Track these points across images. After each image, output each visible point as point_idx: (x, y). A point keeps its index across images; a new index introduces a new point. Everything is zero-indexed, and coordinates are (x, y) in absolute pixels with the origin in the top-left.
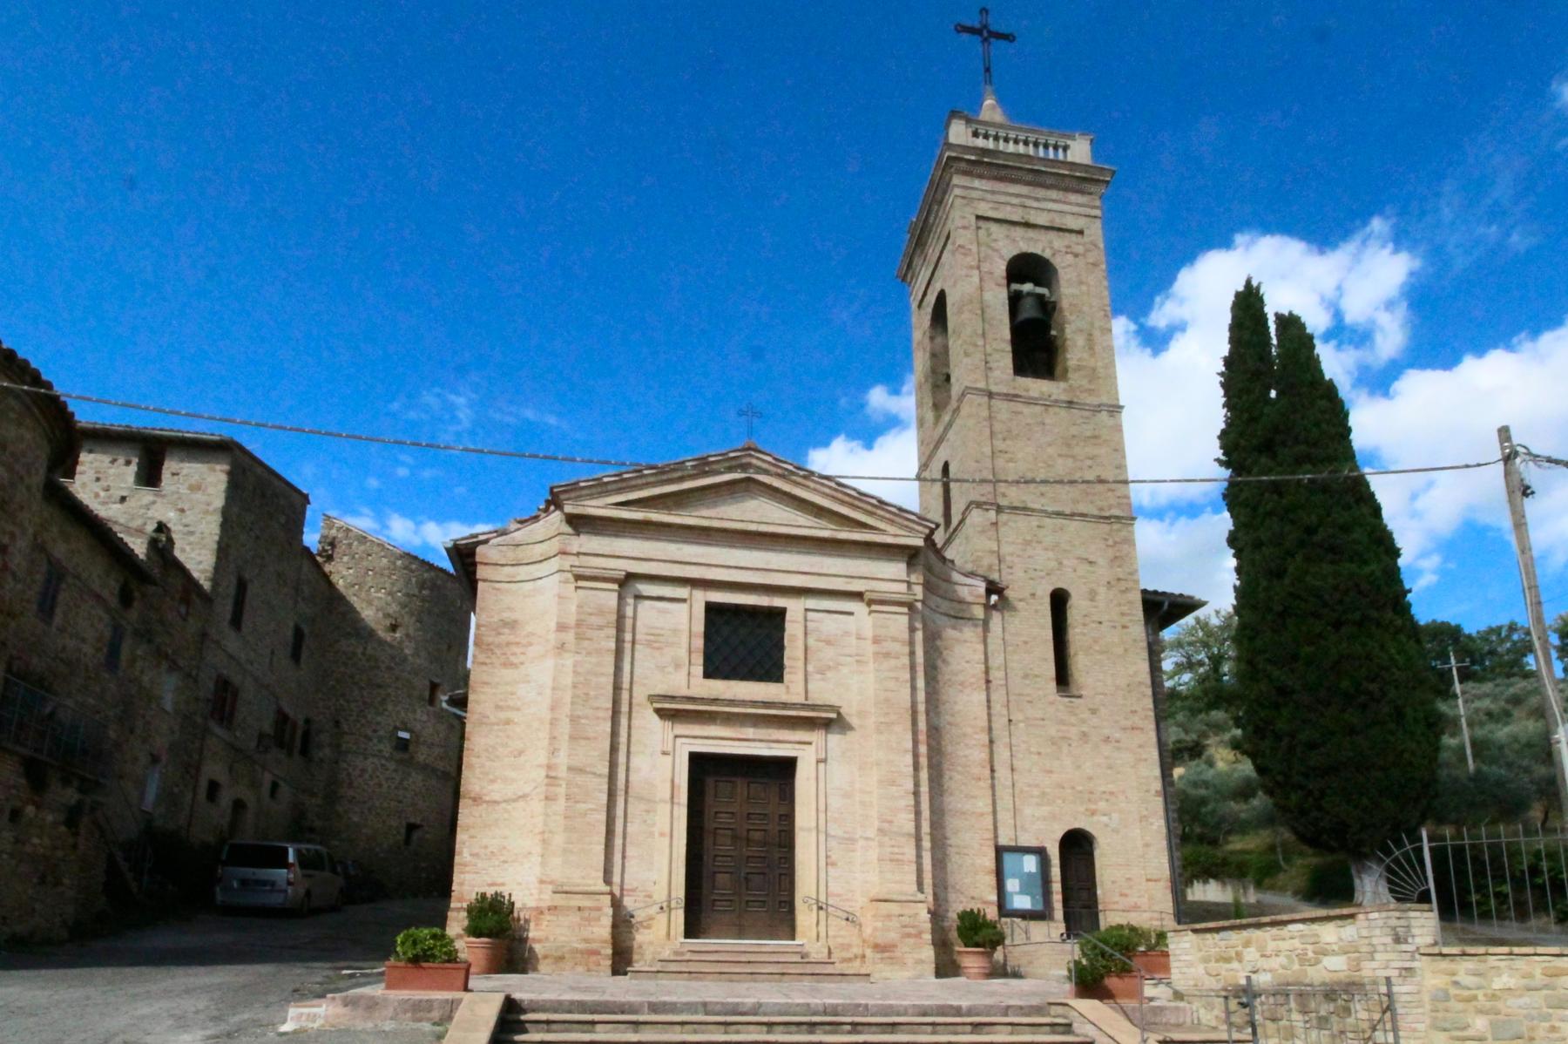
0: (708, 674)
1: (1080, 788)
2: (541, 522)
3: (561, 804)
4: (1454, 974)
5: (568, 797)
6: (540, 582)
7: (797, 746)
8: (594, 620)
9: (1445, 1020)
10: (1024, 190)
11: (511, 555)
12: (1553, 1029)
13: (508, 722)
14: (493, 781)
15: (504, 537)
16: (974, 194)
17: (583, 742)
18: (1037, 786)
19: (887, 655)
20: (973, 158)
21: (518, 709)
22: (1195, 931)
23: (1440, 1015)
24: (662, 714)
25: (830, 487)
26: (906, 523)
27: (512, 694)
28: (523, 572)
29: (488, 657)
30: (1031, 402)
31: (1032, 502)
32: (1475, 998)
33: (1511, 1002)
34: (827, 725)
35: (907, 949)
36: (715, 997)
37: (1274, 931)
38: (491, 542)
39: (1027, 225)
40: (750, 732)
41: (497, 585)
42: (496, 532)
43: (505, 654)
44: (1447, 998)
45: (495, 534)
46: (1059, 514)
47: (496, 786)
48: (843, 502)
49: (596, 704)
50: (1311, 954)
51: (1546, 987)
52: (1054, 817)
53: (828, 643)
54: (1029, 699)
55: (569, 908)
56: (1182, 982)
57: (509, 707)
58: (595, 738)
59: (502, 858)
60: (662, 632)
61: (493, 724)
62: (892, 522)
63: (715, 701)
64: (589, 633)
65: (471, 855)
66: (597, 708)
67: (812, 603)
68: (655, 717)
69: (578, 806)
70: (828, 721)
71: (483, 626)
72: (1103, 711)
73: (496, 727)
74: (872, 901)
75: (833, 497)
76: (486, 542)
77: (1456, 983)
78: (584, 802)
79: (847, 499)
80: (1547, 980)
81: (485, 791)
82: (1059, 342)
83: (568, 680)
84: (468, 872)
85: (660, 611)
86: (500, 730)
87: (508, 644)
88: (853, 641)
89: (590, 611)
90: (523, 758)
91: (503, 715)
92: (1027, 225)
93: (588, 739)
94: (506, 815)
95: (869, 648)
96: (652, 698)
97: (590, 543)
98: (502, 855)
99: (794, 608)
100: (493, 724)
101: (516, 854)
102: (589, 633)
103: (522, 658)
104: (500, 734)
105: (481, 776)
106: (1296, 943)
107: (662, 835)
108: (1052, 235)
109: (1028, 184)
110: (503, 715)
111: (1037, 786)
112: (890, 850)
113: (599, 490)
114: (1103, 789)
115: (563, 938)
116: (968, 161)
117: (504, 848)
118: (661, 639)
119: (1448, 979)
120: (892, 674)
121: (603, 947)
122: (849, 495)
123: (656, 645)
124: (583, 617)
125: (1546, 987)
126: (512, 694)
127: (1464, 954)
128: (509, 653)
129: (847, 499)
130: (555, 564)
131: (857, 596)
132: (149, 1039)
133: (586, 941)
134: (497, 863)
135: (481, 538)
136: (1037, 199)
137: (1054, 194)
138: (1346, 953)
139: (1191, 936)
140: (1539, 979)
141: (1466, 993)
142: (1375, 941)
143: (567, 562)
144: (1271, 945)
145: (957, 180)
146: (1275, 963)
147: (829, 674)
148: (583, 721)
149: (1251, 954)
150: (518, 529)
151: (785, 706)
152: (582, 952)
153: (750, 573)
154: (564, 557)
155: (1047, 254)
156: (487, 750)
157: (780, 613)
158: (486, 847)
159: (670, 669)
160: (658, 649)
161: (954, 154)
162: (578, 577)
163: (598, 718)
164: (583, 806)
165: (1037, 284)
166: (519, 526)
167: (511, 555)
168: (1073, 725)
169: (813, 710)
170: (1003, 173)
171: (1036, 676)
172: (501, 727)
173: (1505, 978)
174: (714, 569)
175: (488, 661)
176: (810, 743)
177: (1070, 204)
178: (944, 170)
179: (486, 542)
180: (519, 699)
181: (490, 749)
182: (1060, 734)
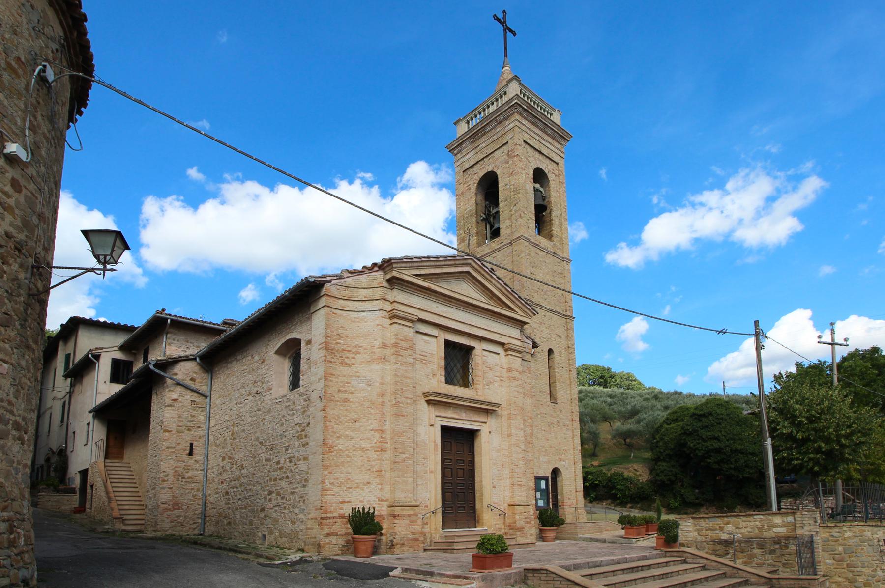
0: (447, 382)
1: (557, 448)
2: (365, 276)
3: (389, 455)
4: (831, 533)
5: (396, 450)
6: (363, 314)
7: (481, 424)
8: (403, 344)
9: (828, 548)
10: (540, 133)
11: (344, 293)
12: (862, 549)
13: (346, 400)
14: (339, 438)
15: (340, 280)
16: (523, 128)
17: (402, 418)
18: (544, 446)
19: (515, 379)
20: (526, 108)
21: (352, 393)
22: (693, 518)
23: (826, 547)
24: (429, 402)
25: (501, 285)
26: (526, 310)
27: (348, 383)
28: (350, 305)
29: (332, 358)
30: (542, 249)
31: (543, 303)
32: (838, 540)
33: (851, 541)
34: (487, 412)
35: (527, 529)
36: (538, 561)
37: (745, 518)
38: (333, 282)
39: (540, 152)
40: (463, 415)
41: (335, 311)
42: (337, 276)
43: (341, 357)
44: (829, 540)
45: (335, 278)
46: (551, 311)
47: (341, 441)
48: (503, 294)
49: (407, 396)
50: (766, 527)
51: (860, 536)
52: (549, 462)
53: (490, 369)
54: (541, 403)
55: (404, 515)
56: (684, 539)
57: (346, 391)
58: (407, 416)
59: (348, 486)
60: (426, 354)
61: (338, 401)
62: (521, 308)
63: (446, 396)
64: (402, 352)
65: (330, 484)
66: (407, 398)
67: (485, 346)
68: (425, 405)
69: (401, 455)
70: (487, 410)
71: (328, 337)
72: (564, 411)
73: (338, 403)
74: (509, 506)
75: (501, 290)
76: (330, 281)
77: (832, 536)
78: (404, 453)
79: (506, 292)
80: (860, 534)
81: (334, 444)
82: (548, 219)
83: (389, 379)
84: (329, 495)
85: (426, 342)
86: (341, 405)
87: (344, 350)
88: (498, 368)
89: (402, 338)
90: (357, 424)
91: (343, 396)
92: (540, 152)
93: (403, 416)
94: (348, 459)
95: (505, 374)
96: (426, 395)
97: (398, 295)
98: (348, 484)
99: (479, 347)
100: (338, 401)
101: (357, 483)
102: (402, 352)
103: (353, 361)
104: (342, 408)
105: (332, 434)
106: (758, 523)
107: (431, 472)
108: (548, 161)
109: (542, 130)
110: (343, 396)
111: (544, 446)
112: (517, 479)
113: (410, 265)
114: (563, 449)
115: (403, 533)
116: (523, 108)
117: (349, 479)
118: (426, 358)
119: (828, 534)
120: (516, 389)
121: (420, 537)
122: (508, 291)
123: (424, 361)
124: (399, 342)
125: (860, 536)
126: (348, 383)
127: (836, 526)
128: (344, 356)
129: (506, 292)
130: (379, 305)
131: (502, 344)
132: (811, 586)
133: (413, 533)
134: (345, 489)
135: (329, 278)
136: (544, 140)
137: (549, 139)
138: (785, 526)
139: (691, 521)
140: (858, 534)
141: (836, 539)
142: (804, 522)
143: (388, 307)
144: (742, 524)
145: (517, 116)
146: (744, 531)
147: (491, 386)
148: (401, 405)
149: (730, 527)
150: (348, 277)
151: (475, 401)
152: (411, 540)
153: (465, 326)
154: (384, 301)
155: (546, 171)
156: (334, 418)
157: (470, 349)
158: (337, 479)
159: (430, 377)
160: (425, 364)
161: (519, 102)
162: (393, 317)
163: (407, 404)
164: (403, 456)
165: (541, 186)
166: (350, 275)
167: (344, 293)
168: (555, 417)
169: (491, 406)
170: (535, 120)
171: (544, 392)
172: (341, 403)
173: (848, 534)
174: (451, 321)
175: (333, 360)
176: (486, 423)
177: (554, 146)
178: (509, 108)
179: (330, 281)
180: (352, 386)
181: (336, 417)
182: (551, 422)
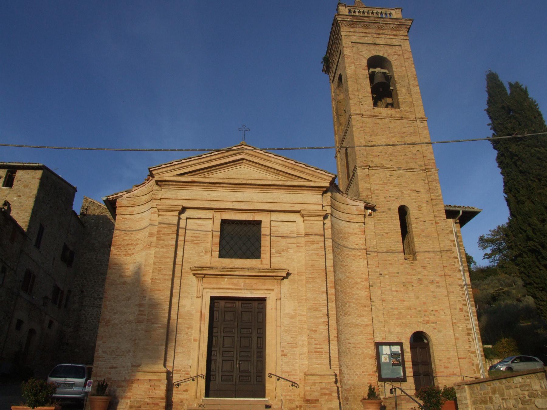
0: (221, 256)
1: (420, 309)
7: (266, 292)
14: (115, 313)
18: (396, 309)
19: (313, 242)
26: (320, 176)
29: (118, 251)
31: (386, 164)
38: (124, 196)
41: (125, 216)
45: (125, 193)
49: (165, 273)
54: (390, 262)
59: (117, 354)
61: (118, 284)
66: (165, 275)
67: (274, 216)
73: (119, 286)
76: (122, 196)
87: (128, 244)
94: (120, 331)
97: (166, 193)
101: (123, 351)
102: (164, 237)
103: (133, 251)
107: (195, 340)
108: (387, 48)
111: (396, 309)
112: (315, 346)
114: (431, 309)
117: (118, 348)
118: (198, 239)
121: (160, 402)
123: (196, 242)
124: (161, 229)
128: (127, 249)
134: (115, 356)
148: (157, 281)
153: (243, 203)
155: (385, 56)
157: (259, 223)
158: (110, 348)
159: (202, 254)
163: (165, 279)
165: (382, 68)
168: (414, 275)
175: (118, 253)
176: (273, 290)
